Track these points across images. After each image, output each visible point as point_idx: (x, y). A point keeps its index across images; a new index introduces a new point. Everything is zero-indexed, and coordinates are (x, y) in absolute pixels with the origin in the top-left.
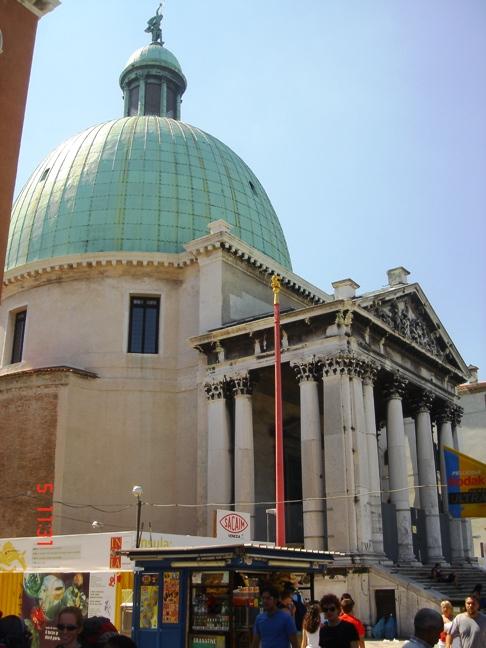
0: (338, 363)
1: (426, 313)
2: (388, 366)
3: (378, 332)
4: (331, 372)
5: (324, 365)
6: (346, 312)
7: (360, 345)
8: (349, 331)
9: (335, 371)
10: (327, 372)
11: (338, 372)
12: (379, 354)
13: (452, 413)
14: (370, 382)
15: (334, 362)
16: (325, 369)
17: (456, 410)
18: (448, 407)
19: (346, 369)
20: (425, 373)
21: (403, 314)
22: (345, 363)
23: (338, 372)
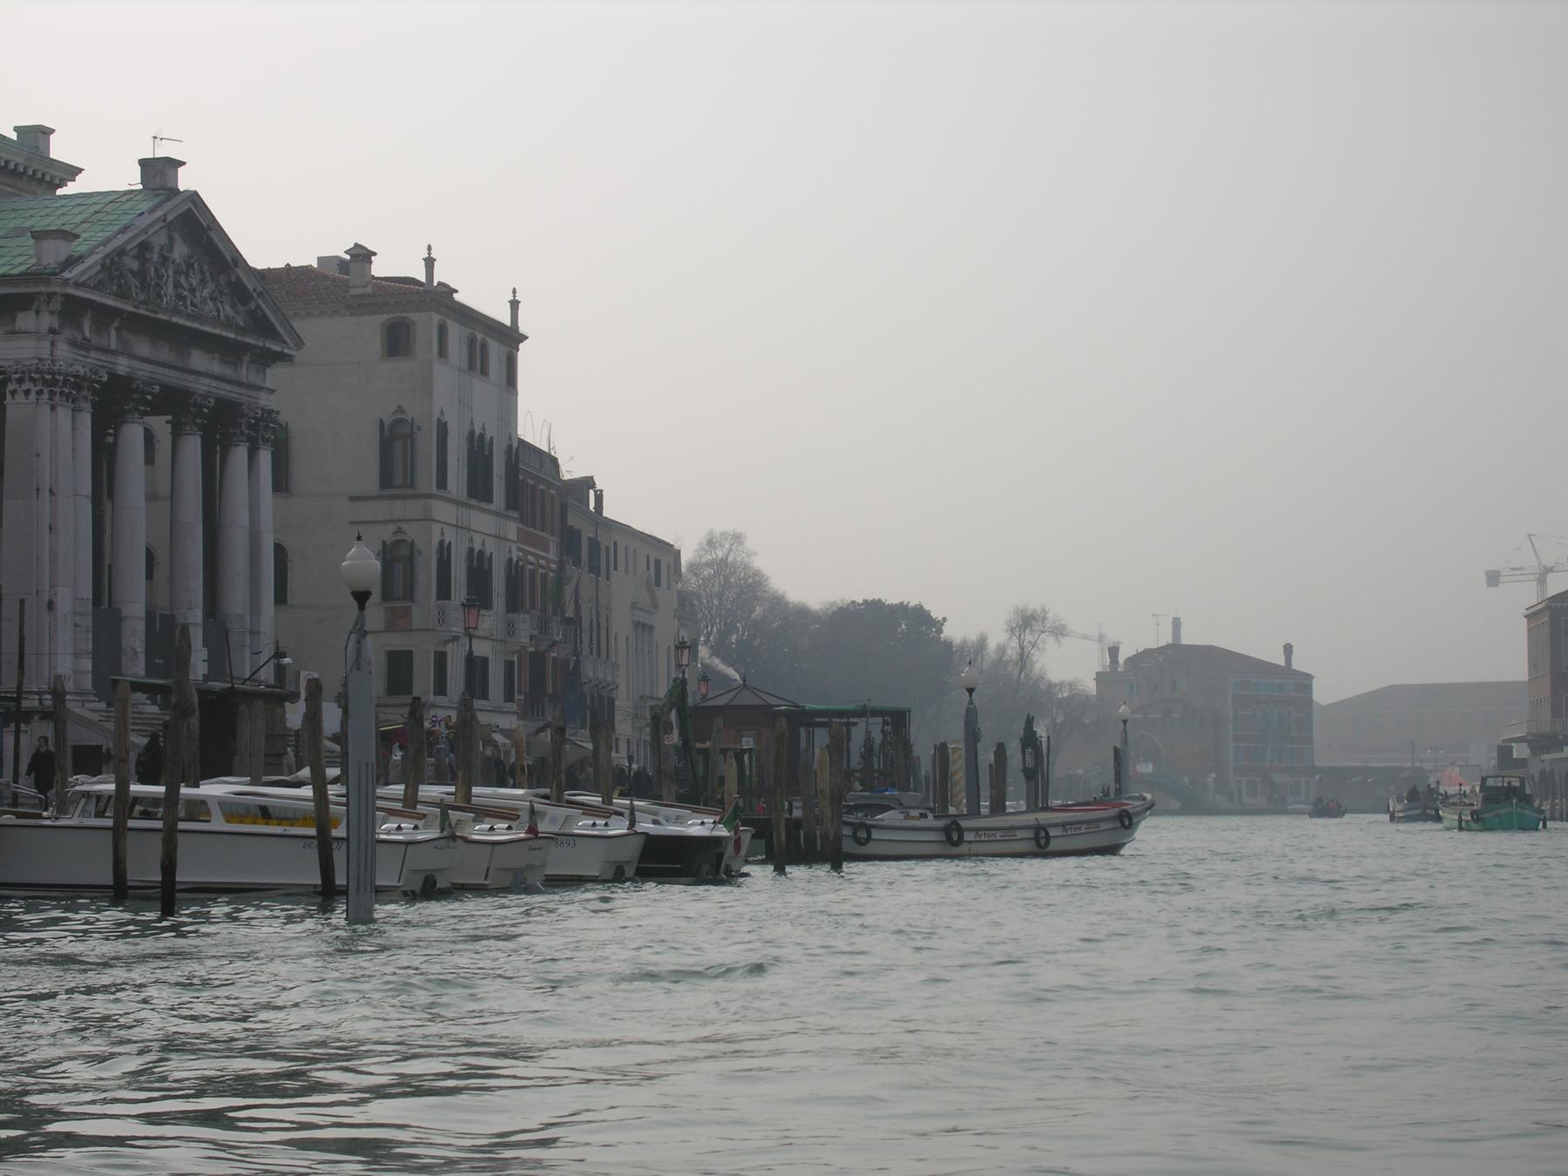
0: (32, 380)
1: (210, 242)
2: (123, 366)
3: (104, 315)
4: (20, 397)
5: (9, 379)
6: (50, 295)
7: (72, 344)
8: (56, 324)
9: (27, 393)
10: (13, 393)
11: (33, 396)
12: (107, 351)
13: (251, 427)
14: (87, 406)
15: (27, 377)
16: (10, 387)
17: (262, 419)
18: (242, 415)
19: (46, 390)
20: (198, 360)
21: (161, 256)
22: (45, 381)
23: (33, 396)
